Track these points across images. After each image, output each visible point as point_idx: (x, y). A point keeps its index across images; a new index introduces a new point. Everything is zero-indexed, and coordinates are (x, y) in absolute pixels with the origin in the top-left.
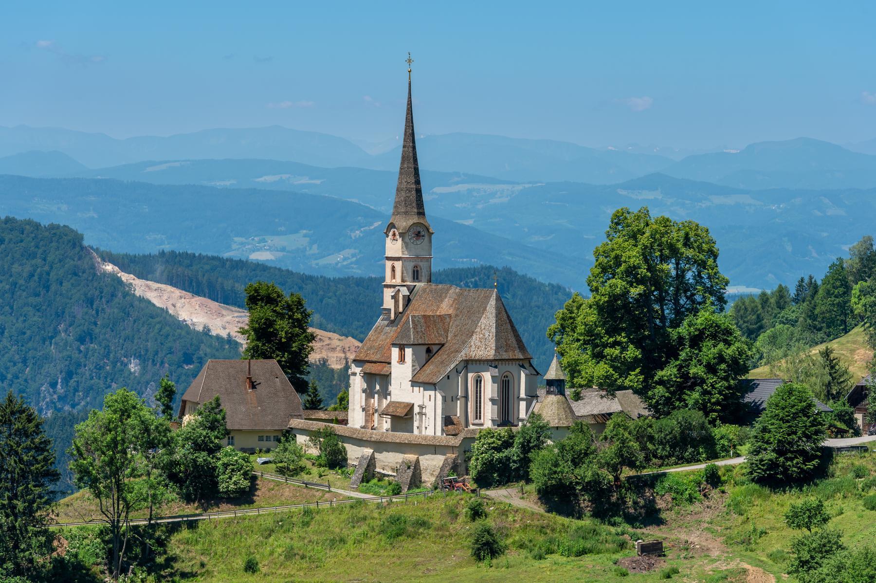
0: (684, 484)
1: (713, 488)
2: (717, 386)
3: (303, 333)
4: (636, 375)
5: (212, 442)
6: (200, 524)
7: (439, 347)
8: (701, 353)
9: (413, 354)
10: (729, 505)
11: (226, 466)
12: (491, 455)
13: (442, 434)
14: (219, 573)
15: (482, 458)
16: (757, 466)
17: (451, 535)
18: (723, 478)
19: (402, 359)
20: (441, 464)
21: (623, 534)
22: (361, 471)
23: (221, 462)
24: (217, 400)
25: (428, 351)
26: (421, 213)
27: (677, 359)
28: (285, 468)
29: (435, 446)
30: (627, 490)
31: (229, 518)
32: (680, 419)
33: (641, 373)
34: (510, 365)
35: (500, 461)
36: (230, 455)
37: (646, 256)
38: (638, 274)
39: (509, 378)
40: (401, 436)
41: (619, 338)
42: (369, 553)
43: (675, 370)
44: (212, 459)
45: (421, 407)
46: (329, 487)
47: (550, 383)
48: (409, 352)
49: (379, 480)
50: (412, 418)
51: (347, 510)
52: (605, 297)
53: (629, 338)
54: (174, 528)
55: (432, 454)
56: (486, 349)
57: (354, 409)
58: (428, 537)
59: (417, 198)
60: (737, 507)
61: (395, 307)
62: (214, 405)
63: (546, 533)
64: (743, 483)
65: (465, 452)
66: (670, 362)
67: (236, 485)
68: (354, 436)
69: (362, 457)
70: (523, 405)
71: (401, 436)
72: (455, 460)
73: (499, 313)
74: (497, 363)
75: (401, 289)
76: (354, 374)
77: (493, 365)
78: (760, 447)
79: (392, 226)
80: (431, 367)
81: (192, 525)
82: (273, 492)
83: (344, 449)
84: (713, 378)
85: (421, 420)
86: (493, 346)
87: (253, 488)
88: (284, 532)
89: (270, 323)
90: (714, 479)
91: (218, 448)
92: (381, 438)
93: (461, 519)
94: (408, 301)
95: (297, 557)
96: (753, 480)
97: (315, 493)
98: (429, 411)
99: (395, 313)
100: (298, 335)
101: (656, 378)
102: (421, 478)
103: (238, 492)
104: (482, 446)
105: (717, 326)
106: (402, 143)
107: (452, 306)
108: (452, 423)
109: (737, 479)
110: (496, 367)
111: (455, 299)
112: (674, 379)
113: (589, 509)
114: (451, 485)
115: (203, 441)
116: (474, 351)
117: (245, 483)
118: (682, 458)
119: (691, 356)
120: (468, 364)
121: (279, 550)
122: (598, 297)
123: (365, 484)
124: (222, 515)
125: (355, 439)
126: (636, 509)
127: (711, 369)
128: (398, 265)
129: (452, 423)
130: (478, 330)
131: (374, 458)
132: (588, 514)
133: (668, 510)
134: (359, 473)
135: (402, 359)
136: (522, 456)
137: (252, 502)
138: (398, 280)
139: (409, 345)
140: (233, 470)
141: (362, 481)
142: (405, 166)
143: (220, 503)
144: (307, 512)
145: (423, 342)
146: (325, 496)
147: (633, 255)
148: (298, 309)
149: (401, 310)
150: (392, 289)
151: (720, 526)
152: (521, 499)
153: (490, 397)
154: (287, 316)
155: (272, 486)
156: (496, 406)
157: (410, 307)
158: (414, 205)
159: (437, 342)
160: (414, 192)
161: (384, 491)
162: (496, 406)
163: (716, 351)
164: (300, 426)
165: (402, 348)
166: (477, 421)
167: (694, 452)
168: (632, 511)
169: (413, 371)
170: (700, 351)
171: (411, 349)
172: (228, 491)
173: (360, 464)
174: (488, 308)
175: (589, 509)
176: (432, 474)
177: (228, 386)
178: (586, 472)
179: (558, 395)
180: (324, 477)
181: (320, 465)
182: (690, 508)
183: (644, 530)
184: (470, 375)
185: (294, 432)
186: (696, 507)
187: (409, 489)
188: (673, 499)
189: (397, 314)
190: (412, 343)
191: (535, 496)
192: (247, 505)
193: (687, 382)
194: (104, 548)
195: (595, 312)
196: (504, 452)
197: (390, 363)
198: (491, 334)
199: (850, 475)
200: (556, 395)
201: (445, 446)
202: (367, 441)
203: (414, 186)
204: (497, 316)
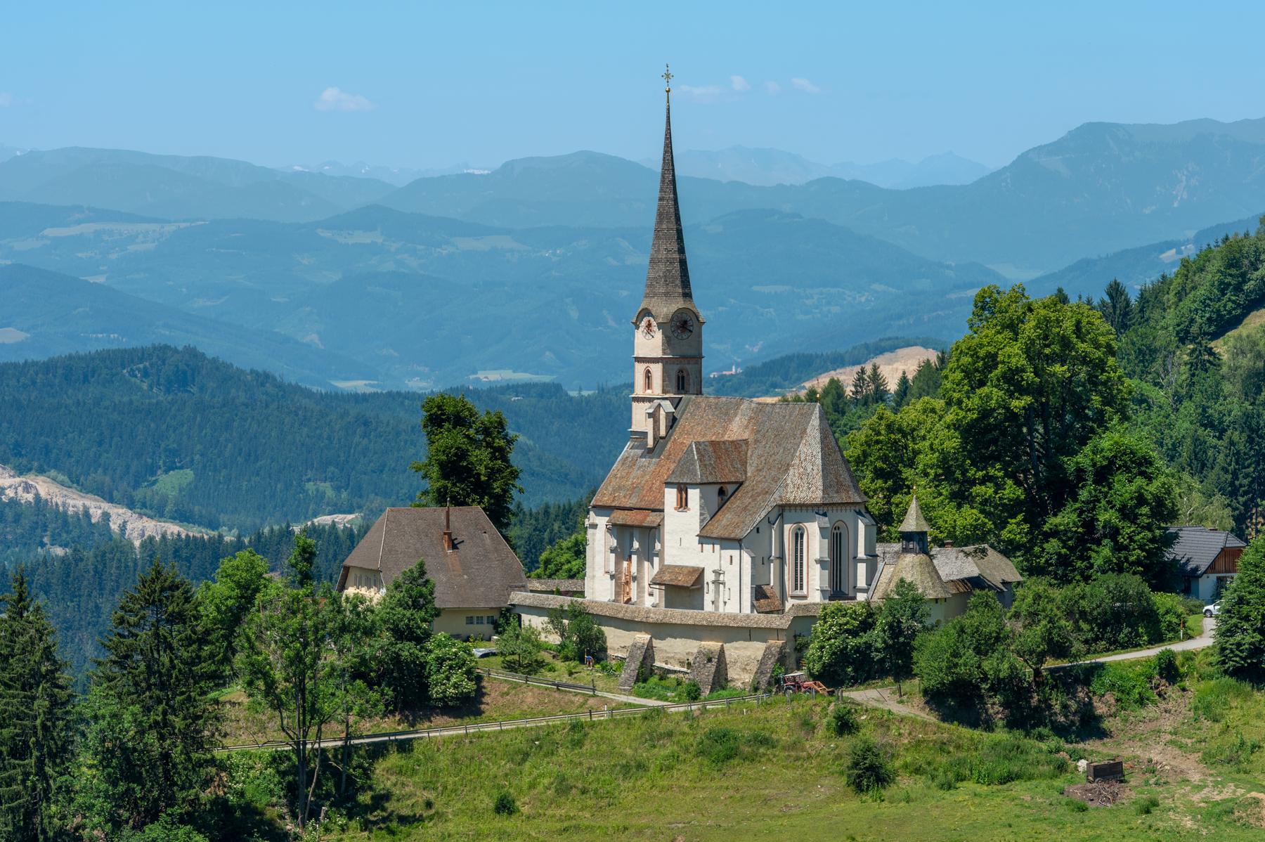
0: (1129, 679)
1: (1170, 684)
2: (1136, 538)
3: (507, 467)
4: (1018, 524)
5: (419, 628)
6: (415, 745)
7: (736, 486)
8: (1112, 492)
9: (701, 498)
10: (1196, 708)
11: (440, 661)
12: (843, 641)
13: (752, 612)
14: (455, 815)
15: (831, 645)
16: (1232, 652)
17: (809, 757)
18: (1182, 670)
19: (683, 504)
20: (760, 655)
21: (1058, 751)
22: (635, 665)
23: (433, 656)
24: (421, 565)
25: (721, 492)
26: (687, 295)
27: (1075, 500)
28: (514, 663)
29: (750, 629)
30: (1052, 689)
31: (457, 736)
32: (1112, 586)
33: (1025, 521)
34: (844, 511)
35: (857, 649)
36: (445, 646)
37: (1031, 354)
38: (1023, 380)
39: (841, 530)
41: (992, 472)
42: (687, 784)
43: (1074, 517)
44: (420, 651)
45: (717, 573)
46: (594, 690)
47: (907, 537)
48: (694, 495)
49: (661, 679)
50: (702, 588)
51: (638, 723)
52: (973, 414)
53: (1006, 471)
54: (378, 751)
55: (745, 640)
56: (810, 489)
57: (594, 576)
58: (774, 760)
59: (681, 272)
60: (1206, 710)
61: (654, 429)
62: (416, 574)
63: (949, 752)
64: (1211, 677)
65: (795, 636)
66: (1065, 505)
67: (457, 688)
68: (620, 616)
69: (634, 645)
72: (782, 648)
73: (826, 438)
74: (825, 509)
75: (663, 403)
76: (594, 526)
77: (821, 512)
78: (1236, 626)
79: (646, 312)
80: (729, 516)
81: (405, 747)
82: (508, 697)
83: (602, 633)
84: (1130, 527)
85: (717, 592)
86: (820, 484)
87: (480, 693)
88: (546, 755)
89: (462, 454)
90: (1169, 671)
91: (427, 635)
92: (664, 618)
93: (820, 732)
94: (673, 421)
95: (574, 791)
96: (1226, 672)
97: (573, 698)
98: (730, 578)
99: (654, 439)
100: (499, 471)
101: (1046, 528)
102: (727, 674)
103: (457, 699)
104: (830, 629)
105: (1132, 453)
106: (657, 195)
107: (747, 427)
108: (765, 596)
109: (1202, 671)
110: (825, 515)
111: (751, 418)
112: (1074, 529)
113: (1000, 716)
115: (407, 625)
116: (792, 492)
117: (469, 686)
118: (1115, 642)
119: (1096, 496)
120: (784, 510)
121: (546, 781)
122: (962, 414)
123: (640, 684)
125: (622, 620)
126: (1066, 716)
127: (1127, 514)
128: (657, 370)
129: (765, 596)
130: (796, 461)
131: (652, 647)
132: (1000, 723)
133: (1111, 716)
134: (632, 668)
135: (683, 504)
136: (890, 642)
137: (479, 713)
138: (657, 390)
139: (694, 485)
140: (451, 667)
141: (637, 680)
142: (664, 226)
143: (431, 715)
145: (714, 480)
146: (589, 702)
147: (1014, 354)
148: (499, 432)
149: (663, 432)
150: (647, 405)
151: (1189, 738)
152: (899, 702)
153: (818, 557)
154: (484, 444)
155: (506, 689)
156: (827, 571)
157: (678, 429)
158: (678, 282)
159: (733, 479)
160: (677, 265)
161: (673, 694)
162: (827, 571)
163: (1133, 488)
164: (527, 602)
165: (682, 489)
166: (798, 593)
167: (1131, 633)
168: (1062, 719)
169: (702, 521)
170: (1110, 489)
171: (697, 491)
172: (445, 697)
173: (632, 656)
174: (808, 431)
175: (1000, 716)
176: (744, 670)
177: (418, 545)
178: (997, 665)
179: (919, 553)
180: (576, 675)
181: (566, 659)
182: (1144, 713)
183: (1081, 745)
184: (787, 527)
185: (517, 611)
186: (1150, 711)
187: (712, 691)
188: (1117, 700)
189: (657, 439)
190: (699, 481)
191: (919, 700)
192: (472, 718)
193: (1088, 535)
194: (279, 783)
195: (956, 434)
196: (862, 637)
197: (662, 511)
198: (815, 468)
200: (917, 554)
201: (765, 628)
202: (641, 622)
203: (676, 256)
204: (822, 442)
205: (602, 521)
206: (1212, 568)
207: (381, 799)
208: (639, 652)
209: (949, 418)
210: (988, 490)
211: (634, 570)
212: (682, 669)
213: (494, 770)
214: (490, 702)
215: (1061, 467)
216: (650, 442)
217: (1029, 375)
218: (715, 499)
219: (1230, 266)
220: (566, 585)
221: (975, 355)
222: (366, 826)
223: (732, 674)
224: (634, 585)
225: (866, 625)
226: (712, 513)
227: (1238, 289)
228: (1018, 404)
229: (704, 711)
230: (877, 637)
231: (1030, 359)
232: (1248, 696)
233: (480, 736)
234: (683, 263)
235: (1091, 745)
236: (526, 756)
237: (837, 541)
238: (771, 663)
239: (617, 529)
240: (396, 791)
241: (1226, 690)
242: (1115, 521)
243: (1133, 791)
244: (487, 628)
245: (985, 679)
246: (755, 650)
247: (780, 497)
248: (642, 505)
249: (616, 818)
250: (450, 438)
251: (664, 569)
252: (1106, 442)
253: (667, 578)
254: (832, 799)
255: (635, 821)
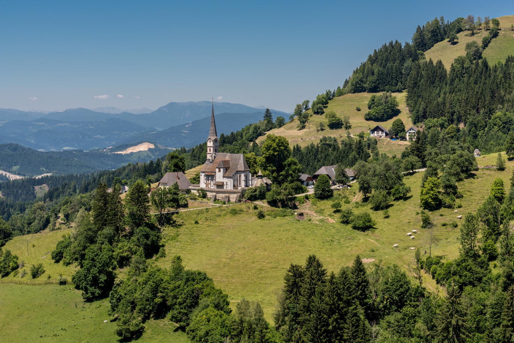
11: (181, 198)
19: (220, 171)
20: (236, 196)
25: (226, 169)
26: (216, 136)
35: (254, 195)
37: (277, 145)
40: (220, 190)
45: (226, 183)
47: (259, 176)
48: (222, 170)
54: (173, 214)
60: (314, 204)
70: (250, 181)
71: (236, 190)
81: (177, 213)
87: (188, 204)
89: (177, 163)
91: (178, 194)
93: (251, 209)
94: (215, 157)
98: (229, 183)
114: (240, 201)
117: (186, 202)
120: (237, 172)
124: (182, 210)
127: (294, 172)
128: (212, 149)
135: (220, 171)
137: (188, 207)
138: (212, 152)
139: (222, 168)
144: (207, 209)
147: (274, 145)
157: (216, 158)
165: (219, 168)
178: (281, 197)
184: (238, 175)
186: (304, 204)
189: (212, 160)
191: (266, 203)
199: (338, 196)
205: (203, 174)
206: (306, 181)
207: (174, 222)
209: (263, 156)
210: (270, 168)
211: (210, 182)
213: (193, 217)
214: (189, 205)
215: (282, 164)
216: (211, 161)
217: (277, 149)
218: (225, 170)
219: (255, 129)
220: (197, 185)
221: (268, 146)
222: (172, 226)
223: (231, 200)
224: (210, 185)
225: (255, 191)
226: (225, 172)
227: (256, 133)
228: (276, 153)
229: (229, 206)
230: (257, 193)
231: (277, 146)
232: (320, 202)
233: (190, 211)
234: (216, 130)
235: (296, 210)
236: (199, 214)
237: (246, 177)
238: (238, 198)
239: (206, 176)
240: (177, 221)
241: (316, 200)
242: (292, 173)
243: (306, 217)
244: (185, 193)
245: (278, 199)
246: (235, 195)
249: (217, 224)
250: (175, 161)
251: (216, 182)
252: (289, 160)
253: (217, 184)
254: (255, 220)
255: (221, 225)
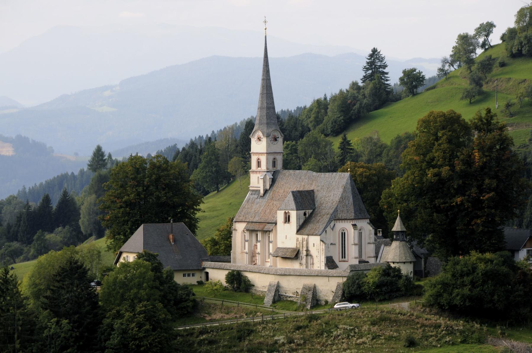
149: (268, 187)
166: (344, 259)
173: (269, 290)
208: (273, 288)
212: (294, 296)
216: (262, 192)
247: (335, 216)
248: (262, 221)
